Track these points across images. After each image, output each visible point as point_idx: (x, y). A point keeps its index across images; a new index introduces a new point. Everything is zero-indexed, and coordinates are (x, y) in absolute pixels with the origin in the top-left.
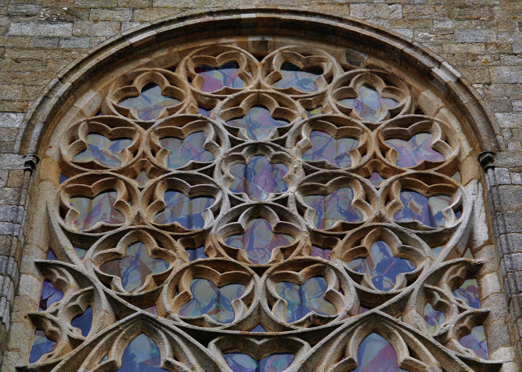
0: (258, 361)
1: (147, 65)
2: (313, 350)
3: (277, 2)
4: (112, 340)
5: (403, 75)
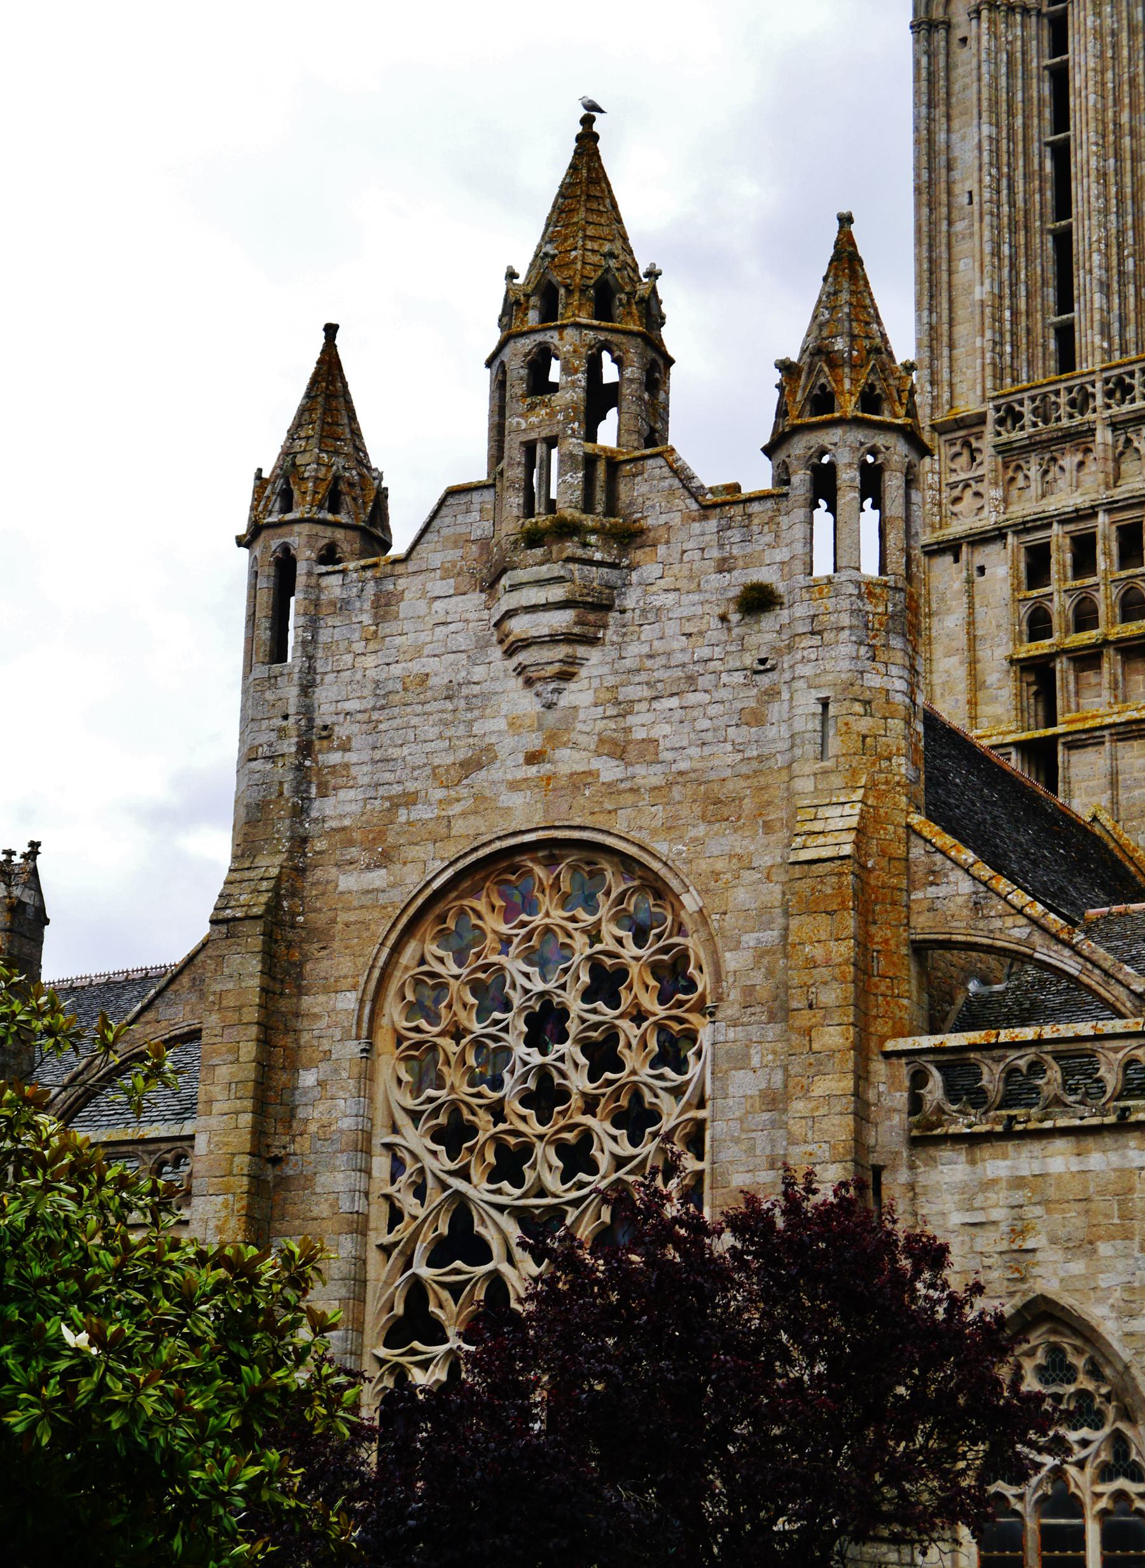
2: (577, 1213)
3: (555, 816)
4: (438, 1213)
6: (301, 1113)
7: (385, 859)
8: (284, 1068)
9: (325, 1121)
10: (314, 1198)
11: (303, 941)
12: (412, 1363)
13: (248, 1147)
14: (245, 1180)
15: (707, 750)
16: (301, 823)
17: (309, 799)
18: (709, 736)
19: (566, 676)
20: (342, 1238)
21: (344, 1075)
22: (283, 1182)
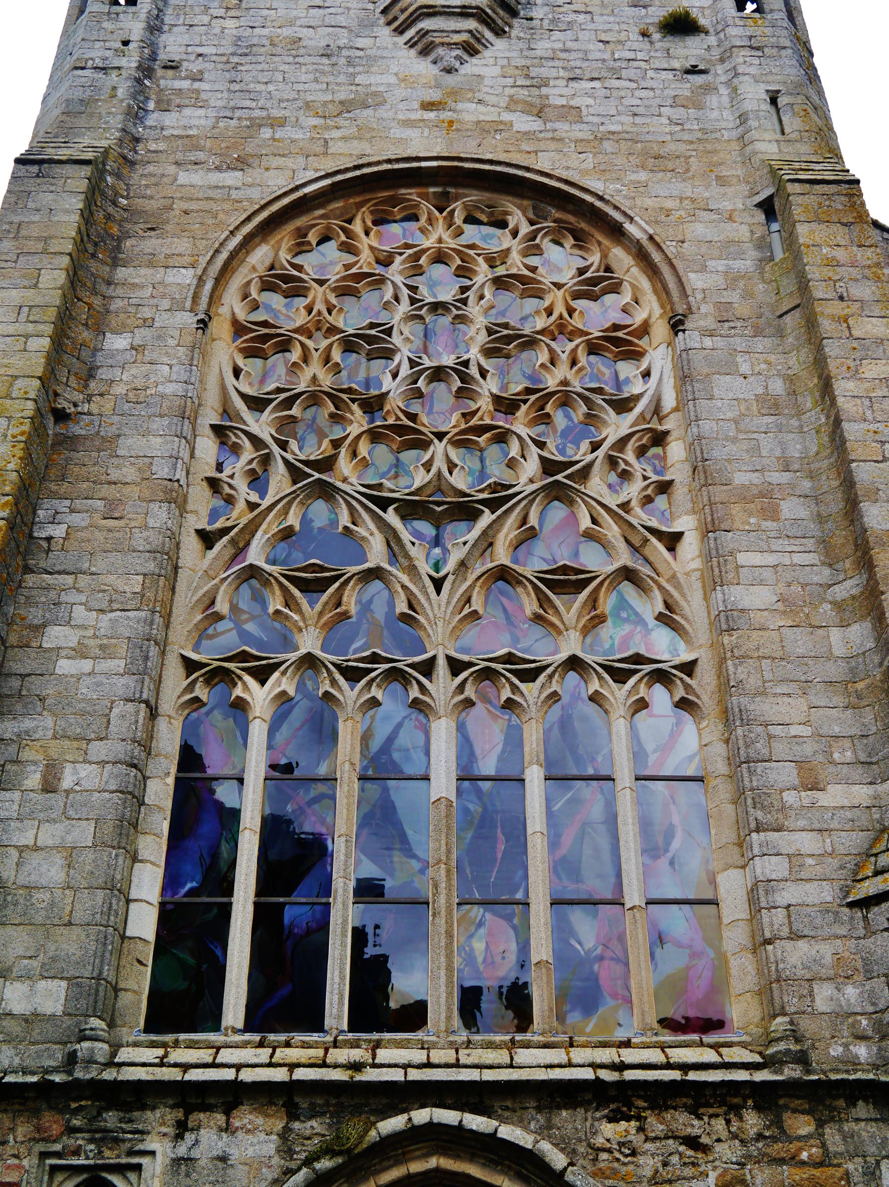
0: (437, 528)
1: (322, 217)
2: (494, 517)
3: (460, 150)
4: (290, 503)
5: (593, 231)
6: (103, 374)
7: (242, 163)
8: (86, 325)
9: (139, 383)
10: (115, 461)
11: (125, 220)
12: (243, 669)
13: (39, 371)
14: (30, 405)
15: (638, 120)
16: (135, 124)
17: (146, 111)
18: (641, 110)
19: (471, 50)
20: (155, 506)
21: (171, 342)
22: (69, 442)
